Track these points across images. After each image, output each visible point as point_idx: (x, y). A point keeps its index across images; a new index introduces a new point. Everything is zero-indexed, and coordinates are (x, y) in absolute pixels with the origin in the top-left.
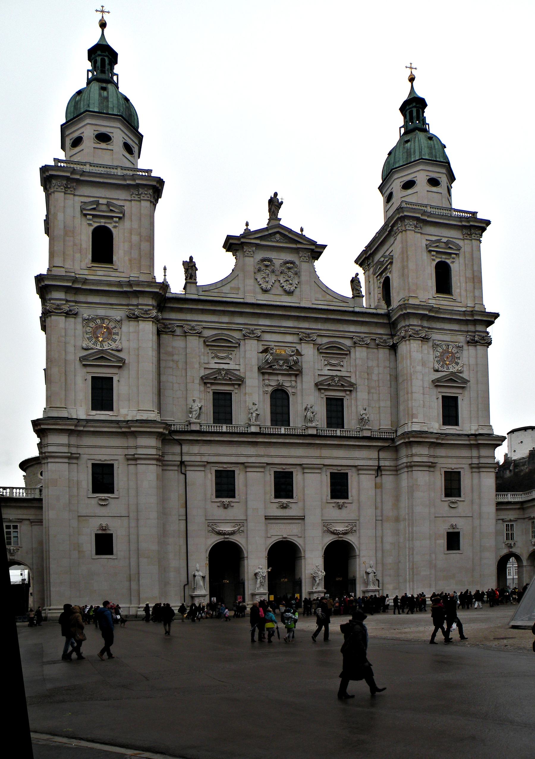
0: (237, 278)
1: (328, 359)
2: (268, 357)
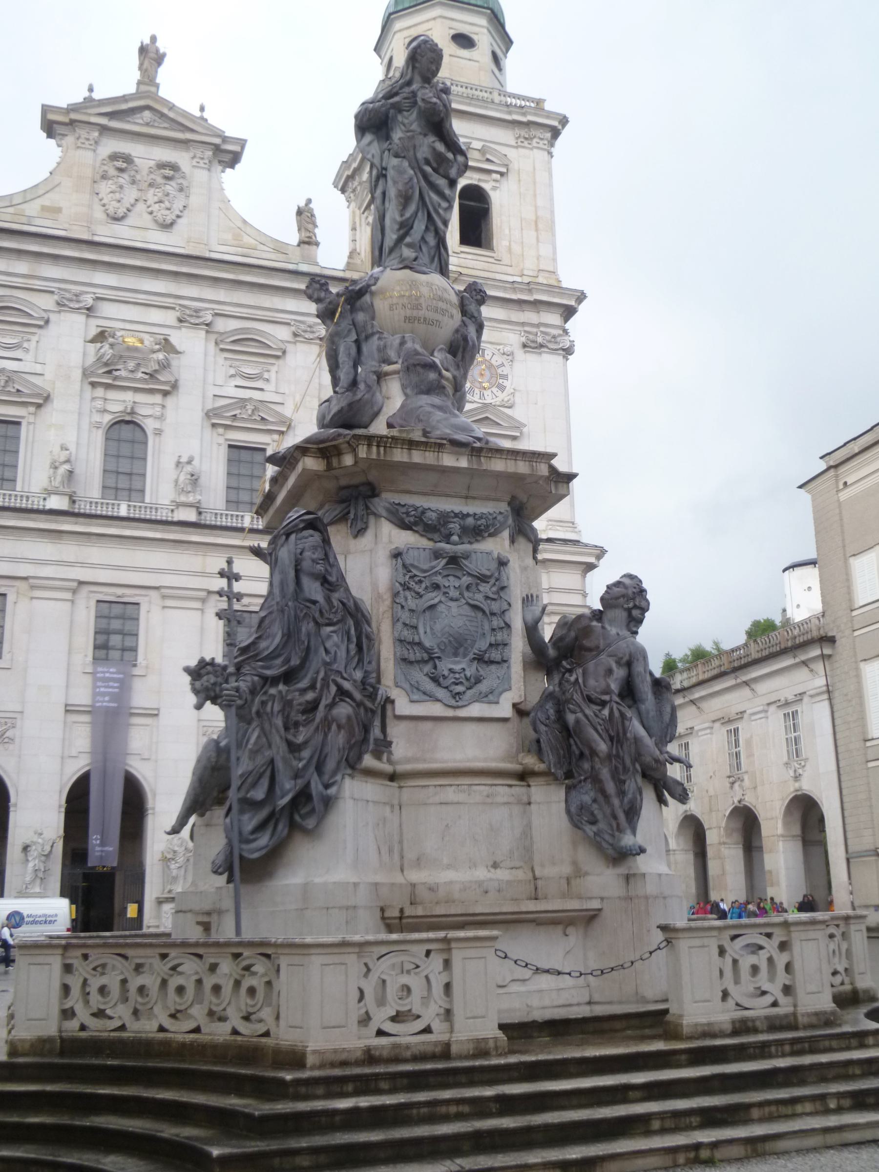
0: (57, 189)
1: (238, 363)
2: (102, 351)
